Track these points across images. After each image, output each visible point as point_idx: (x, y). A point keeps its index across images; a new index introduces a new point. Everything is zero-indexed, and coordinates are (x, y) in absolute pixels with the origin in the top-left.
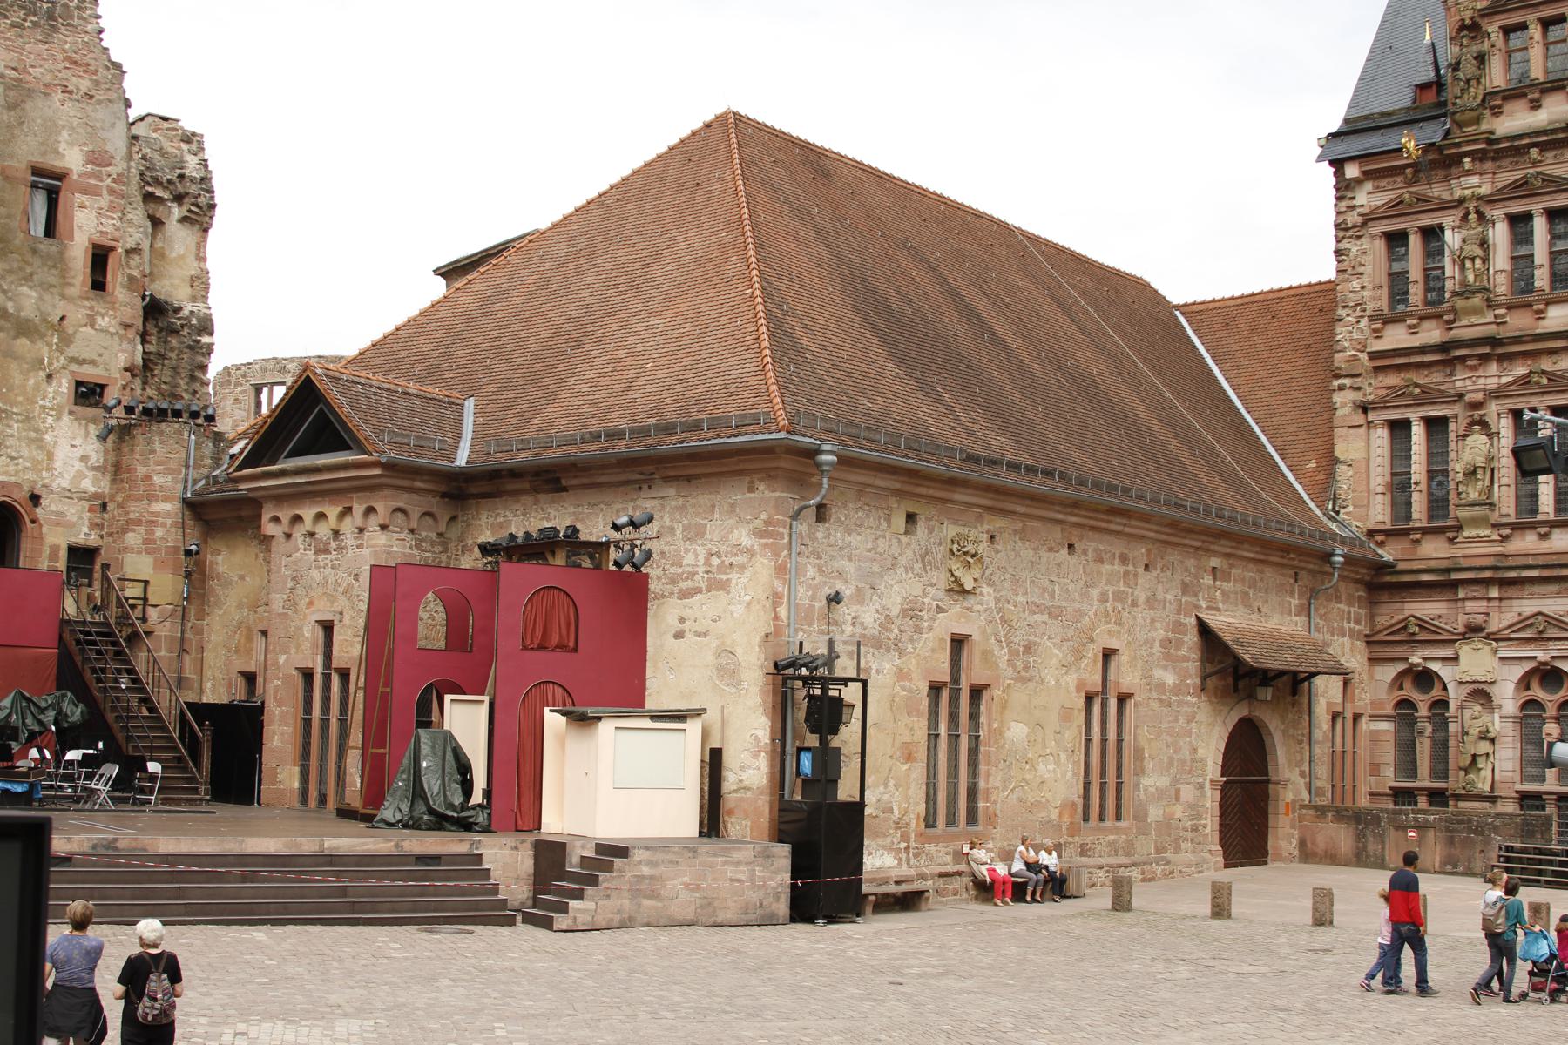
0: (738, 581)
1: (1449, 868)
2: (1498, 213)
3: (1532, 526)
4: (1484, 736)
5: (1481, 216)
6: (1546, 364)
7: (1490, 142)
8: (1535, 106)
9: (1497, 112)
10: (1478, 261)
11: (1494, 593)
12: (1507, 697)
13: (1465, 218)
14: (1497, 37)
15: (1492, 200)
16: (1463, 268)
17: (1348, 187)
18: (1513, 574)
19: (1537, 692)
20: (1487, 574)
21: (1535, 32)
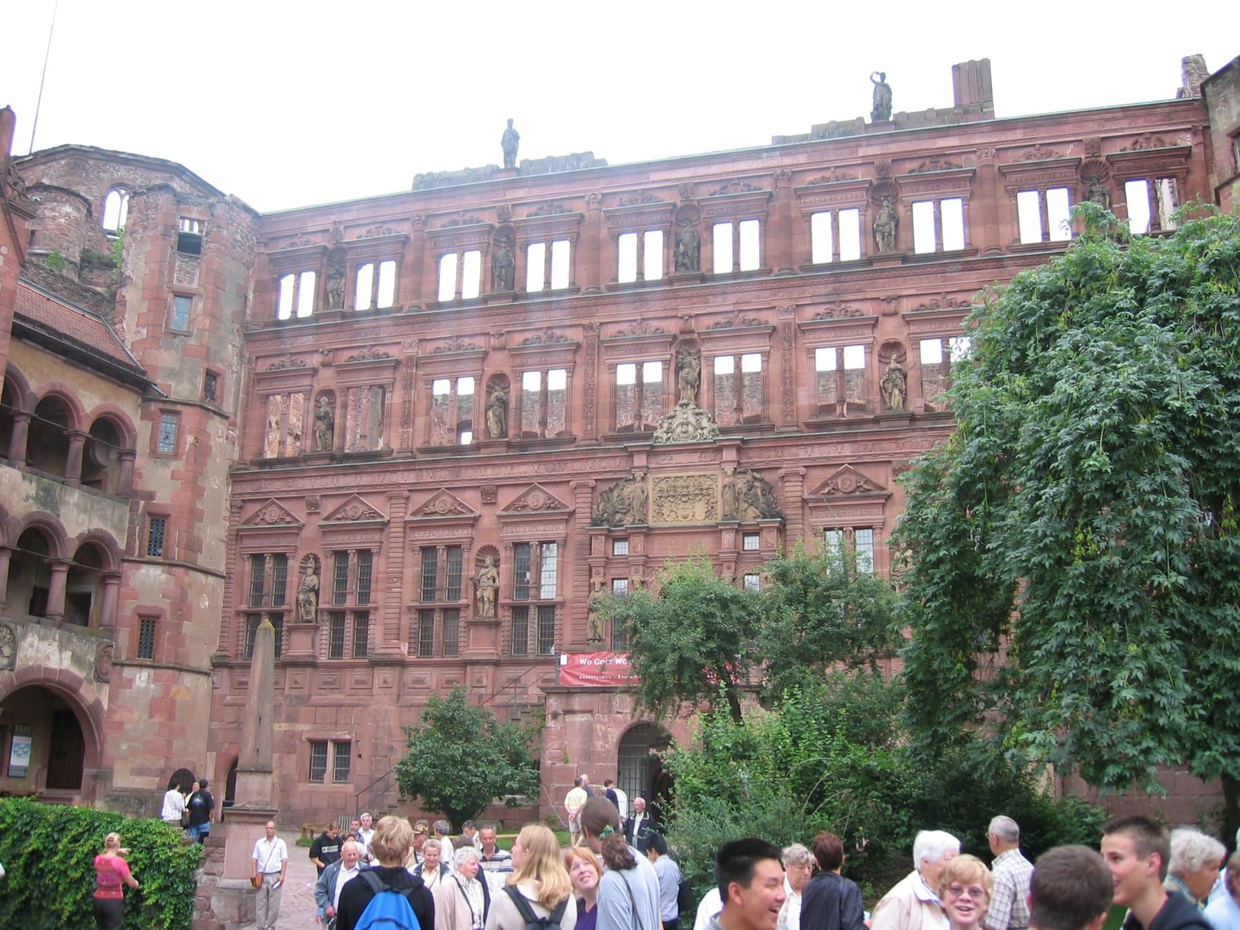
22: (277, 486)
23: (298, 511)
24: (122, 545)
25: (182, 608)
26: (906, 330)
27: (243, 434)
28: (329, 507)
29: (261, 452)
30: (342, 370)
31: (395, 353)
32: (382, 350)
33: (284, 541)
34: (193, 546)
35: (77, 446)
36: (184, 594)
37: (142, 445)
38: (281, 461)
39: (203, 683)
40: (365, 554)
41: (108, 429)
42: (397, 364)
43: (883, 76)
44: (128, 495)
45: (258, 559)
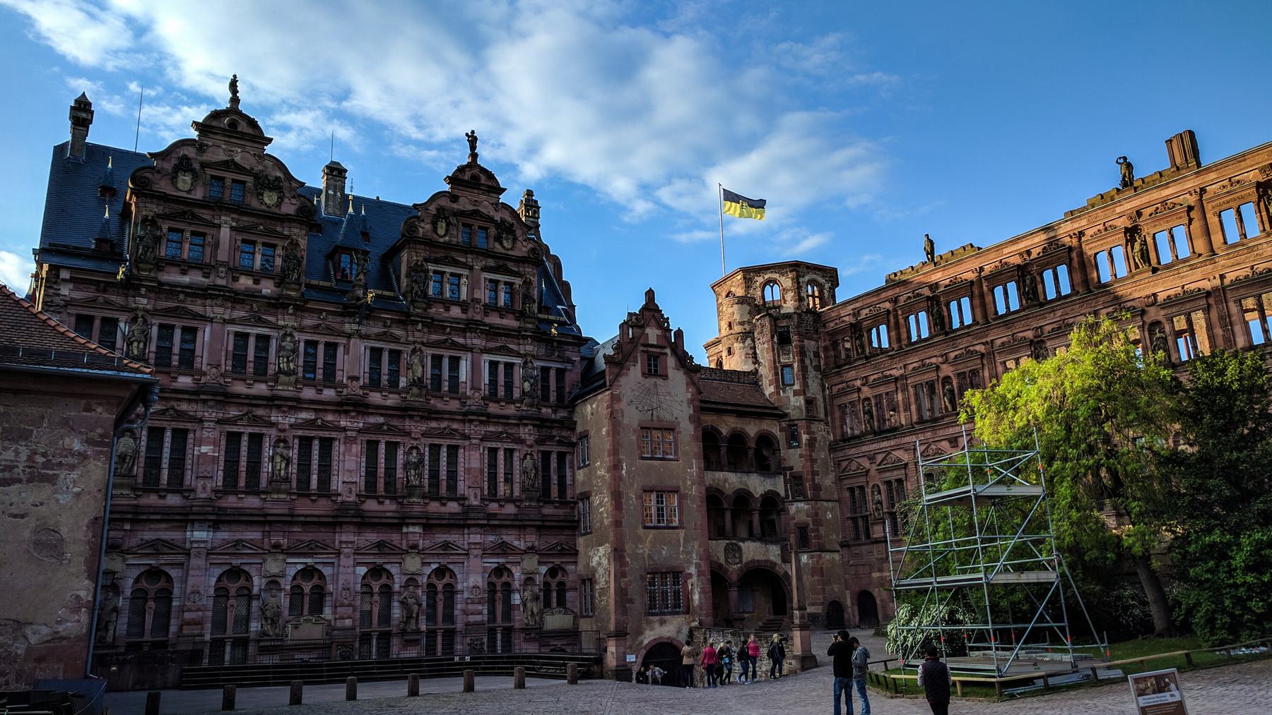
0: (67, 478)
1: (138, 687)
2: (156, 321)
3: (157, 491)
4: (116, 610)
5: (145, 321)
6: (175, 404)
7: (161, 284)
8: (184, 273)
9: (160, 269)
10: (141, 345)
11: (127, 527)
12: (128, 586)
13: (134, 320)
14: (165, 230)
15: (155, 313)
16: (130, 344)
17: (55, 283)
18: (144, 517)
19: (144, 584)
20: (130, 516)
21: (188, 235)
22: (853, 451)
23: (866, 463)
24: (782, 494)
25: (818, 522)
26: (1163, 312)
27: (834, 427)
28: (879, 458)
29: (843, 434)
30: (872, 387)
31: (896, 373)
32: (888, 373)
33: (863, 479)
34: (817, 488)
35: (751, 452)
36: (817, 514)
37: (782, 444)
38: (854, 437)
39: (836, 556)
40: (900, 481)
41: (766, 440)
42: (897, 379)
43: (1125, 159)
44: (781, 470)
45: (851, 490)
